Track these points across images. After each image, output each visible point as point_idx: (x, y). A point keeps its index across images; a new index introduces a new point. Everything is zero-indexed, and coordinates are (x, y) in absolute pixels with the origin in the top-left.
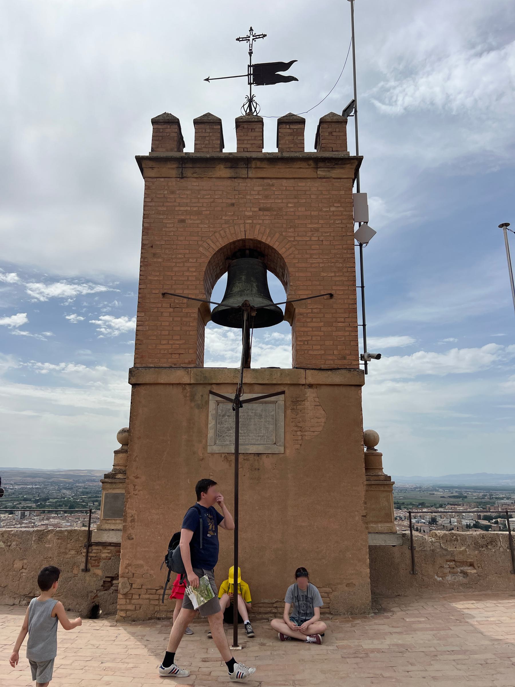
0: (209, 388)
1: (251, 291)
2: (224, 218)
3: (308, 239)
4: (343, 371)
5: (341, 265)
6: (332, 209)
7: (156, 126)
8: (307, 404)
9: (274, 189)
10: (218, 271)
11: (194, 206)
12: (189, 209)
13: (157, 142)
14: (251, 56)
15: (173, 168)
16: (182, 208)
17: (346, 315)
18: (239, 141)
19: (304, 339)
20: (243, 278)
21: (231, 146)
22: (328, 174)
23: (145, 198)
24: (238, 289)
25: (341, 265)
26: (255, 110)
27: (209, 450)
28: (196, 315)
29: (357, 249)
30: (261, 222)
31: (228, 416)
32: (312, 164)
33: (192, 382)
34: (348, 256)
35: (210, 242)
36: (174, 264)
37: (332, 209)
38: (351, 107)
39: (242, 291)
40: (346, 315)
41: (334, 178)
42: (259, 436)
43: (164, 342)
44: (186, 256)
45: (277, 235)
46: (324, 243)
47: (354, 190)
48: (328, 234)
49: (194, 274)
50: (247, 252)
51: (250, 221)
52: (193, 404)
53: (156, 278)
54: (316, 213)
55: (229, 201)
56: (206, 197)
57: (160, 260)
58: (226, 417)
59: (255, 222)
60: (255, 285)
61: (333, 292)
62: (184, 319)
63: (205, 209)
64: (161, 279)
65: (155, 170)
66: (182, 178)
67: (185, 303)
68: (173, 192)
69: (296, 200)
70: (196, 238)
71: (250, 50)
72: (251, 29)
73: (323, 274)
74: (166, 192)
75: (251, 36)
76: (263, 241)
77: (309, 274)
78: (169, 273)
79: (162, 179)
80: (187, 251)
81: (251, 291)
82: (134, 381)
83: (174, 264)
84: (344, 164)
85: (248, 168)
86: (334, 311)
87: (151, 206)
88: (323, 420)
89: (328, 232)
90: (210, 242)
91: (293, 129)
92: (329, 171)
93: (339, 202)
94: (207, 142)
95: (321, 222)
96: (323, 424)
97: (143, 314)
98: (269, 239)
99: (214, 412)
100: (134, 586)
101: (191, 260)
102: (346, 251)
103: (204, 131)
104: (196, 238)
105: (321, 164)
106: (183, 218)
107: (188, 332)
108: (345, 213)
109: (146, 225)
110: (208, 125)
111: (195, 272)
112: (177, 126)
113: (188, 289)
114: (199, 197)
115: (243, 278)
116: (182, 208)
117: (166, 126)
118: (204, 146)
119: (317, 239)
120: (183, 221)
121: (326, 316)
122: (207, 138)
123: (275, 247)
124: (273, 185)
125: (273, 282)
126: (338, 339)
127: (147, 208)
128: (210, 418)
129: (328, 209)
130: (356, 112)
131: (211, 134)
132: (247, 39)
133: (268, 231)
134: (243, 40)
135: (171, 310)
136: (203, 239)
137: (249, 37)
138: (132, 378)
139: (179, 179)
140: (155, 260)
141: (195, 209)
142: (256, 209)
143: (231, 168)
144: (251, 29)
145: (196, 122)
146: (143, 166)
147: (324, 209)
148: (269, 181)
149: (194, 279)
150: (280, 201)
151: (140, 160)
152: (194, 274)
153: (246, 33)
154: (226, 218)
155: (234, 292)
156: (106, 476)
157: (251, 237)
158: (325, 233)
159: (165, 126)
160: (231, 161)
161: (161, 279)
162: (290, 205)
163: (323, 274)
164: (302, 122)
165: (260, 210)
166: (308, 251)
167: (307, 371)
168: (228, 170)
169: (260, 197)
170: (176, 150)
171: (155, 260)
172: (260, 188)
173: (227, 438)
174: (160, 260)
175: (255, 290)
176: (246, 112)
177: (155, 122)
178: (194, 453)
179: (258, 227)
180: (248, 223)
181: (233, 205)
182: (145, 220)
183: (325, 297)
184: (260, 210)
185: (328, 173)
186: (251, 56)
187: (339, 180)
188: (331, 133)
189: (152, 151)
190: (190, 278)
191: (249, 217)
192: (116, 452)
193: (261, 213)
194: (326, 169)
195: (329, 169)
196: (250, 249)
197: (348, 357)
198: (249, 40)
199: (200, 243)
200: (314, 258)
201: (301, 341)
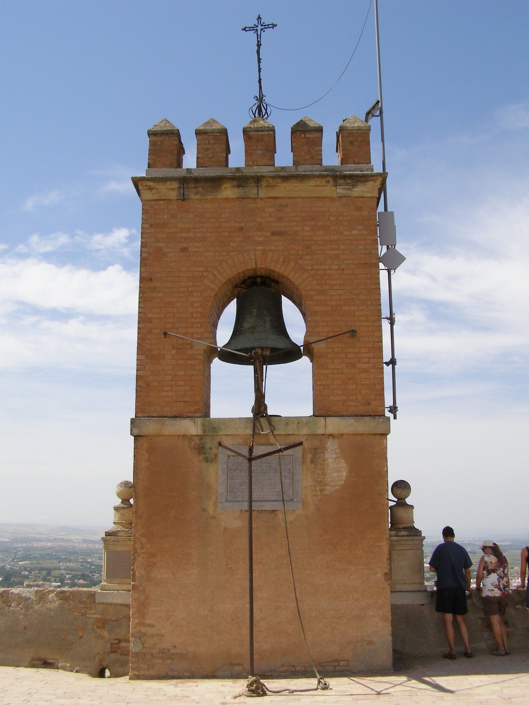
1: (264, 327)
2: (231, 244)
3: (327, 267)
4: (367, 419)
5: (365, 297)
7: (153, 138)
8: (327, 455)
9: (288, 210)
10: (225, 300)
11: (197, 232)
12: (192, 235)
13: (154, 157)
14: (260, 99)
15: (174, 189)
16: (185, 235)
17: (371, 355)
18: (248, 153)
19: (324, 383)
20: (255, 311)
21: (237, 159)
23: (142, 224)
24: (249, 325)
25: (365, 297)
26: (266, 112)
28: (201, 357)
29: (383, 275)
30: (273, 248)
31: (240, 470)
32: (331, 180)
33: (200, 432)
34: (373, 287)
35: (216, 272)
36: (177, 299)
37: (355, 232)
38: (375, 110)
39: (254, 328)
40: (371, 355)
41: (356, 197)
42: (274, 492)
43: (168, 388)
44: (190, 289)
45: (292, 263)
46: (346, 272)
47: (381, 208)
48: (350, 262)
49: (199, 310)
50: (259, 280)
51: (261, 248)
52: (201, 457)
53: (156, 316)
54: (336, 237)
55: (237, 225)
56: (211, 221)
57: (160, 295)
58: (238, 471)
59: (266, 248)
60: (268, 319)
61: (357, 328)
62: (189, 362)
63: (209, 235)
64: (163, 316)
65: (154, 191)
66: (183, 200)
67: (189, 344)
68: (174, 217)
70: (201, 269)
71: (258, 42)
72: (259, 18)
73: (345, 308)
74: (166, 217)
75: (259, 25)
76: (277, 270)
77: (329, 308)
79: (162, 202)
80: (191, 284)
81: (264, 327)
82: (136, 432)
83: (177, 299)
84: (367, 181)
85: (258, 186)
86: (358, 351)
87: (149, 233)
88: (345, 474)
89: (349, 259)
90: (216, 272)
91: (308, 138)
92: (350, 189)
94: (211, 155)
95: (342, 247)
96: (344, 478)
97: (143, 357)
98: (284, 268)
99: (225, 466)
100: (146, 645)
102: (370, 282)
103: (207, 142)
104: (201, 269)
105: (341, 181)
106: (185, 245)
107: (193, 377)
108: (368, 237)
109: (145, 255)
110: (214, 139)
111: (199, 307)
112: (176, 138)
113: (192, 327)
114: (203, 220)
115: (255, 311)
116: (185, 235)
117: (165, 143)
118: (208, 159)
119: (337, 267)
120: (185, 250)
121: (348, 357)
122: (211, 151)
123: (290, 277)
124: (287, 206)
125: (290, 311)
126: (362, 383)
127: (144, 236)
128: (220, 472)
129: (349, 233)
130: (381, 113)
131: (215, 146)
132: (253, 29)
133: (282, 259)
134: (250, 30)
135: (174, 351)
136: (208, 270)
137: (257, 26)
138: (134, 429)
139: (180, 201)
140: (155, 295)
141: (198, 235)
142: (269, 234)
143: (239, 186)
144: (259, 18)
145: (198, 133)
146: (140, 187)
147: (345, 233)
148: (282, 201)
149: (199, 315)
150: (295, 224)
151: (136, 181)
152: (199, 310)
153: (253, 22)
154: (234, 245)
155: (243, 329)
156: (108, 534)
157: (263, 266)
158: (346, 259)
159: (163, 138)
160: (240, 179)
161: (163, 316)
162: (306, 229)
163: (345, 308)
164: (320, 130)
165: (272, 234)
166: (327, 282)
167: (328, 419)
168: (236, 190)
169: (272, 220)
170: (176, 165)
171: (155, 295)
172: (273, 210)
173: (239, 494)
174: (160, 295)
175: (268, 326)
176: (254, 115)
177: (151, 134)
178: (204, 510)
179: (270, 254)
180: (259, 250)
181: (241, 229)
182: (143, 249)
183: (347, 335)
184: (272, 234)
185: (348, 192)
186: (260, 99)
187: (361, 199)
189: (148, 167)
190: (195, 315)
191: (260, 243)
192: (116, 509)
193: (274, 238)
194: (347, 187)
195: (350, 187)
196: (261, 277)
197: (372, 402)
198: (257, 30)
199: (205, 274)
200: (334, 290)
201: (320, 385)
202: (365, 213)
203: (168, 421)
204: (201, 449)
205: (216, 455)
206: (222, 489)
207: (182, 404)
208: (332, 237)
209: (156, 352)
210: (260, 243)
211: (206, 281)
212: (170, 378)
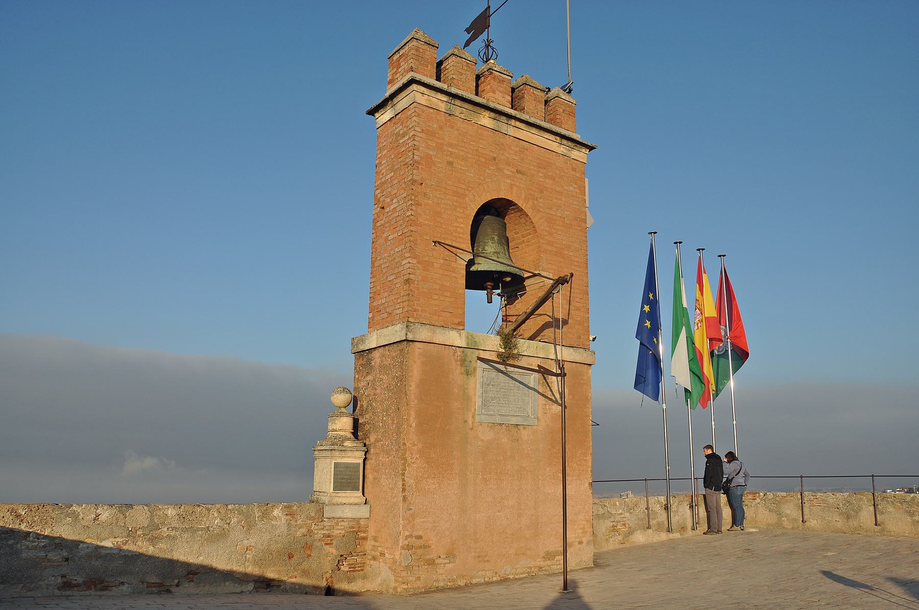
0: (476, 353)
6: (571, 188)
20: (496, 238)
22: (568, 154)
27: (477, 418)
37: (571, 188)
43: (436, 297)
55: (491, 154)
68: (441, 128)
69: (545, 171)
70: (463, 187)
74: (435, 126)
77: (555, 249)
78: (439, 219)
93: (576, 183)
101: (458, 209)
104: (463, 187)
120: (450, 163)
128: (478, 386)
181: (494, 159)
188: (564, 111)
193: (519, 175)
199: (467, 192)
202: (578, 175)
203: (438, 330)
204: (463, 362)
205: (475, 369)
206: (478, 402)
207: (448, 315)
208: (557, 189)
209: (427, 259)
210: (508, 177)
211: (467, 198)
212: (437, 287)
